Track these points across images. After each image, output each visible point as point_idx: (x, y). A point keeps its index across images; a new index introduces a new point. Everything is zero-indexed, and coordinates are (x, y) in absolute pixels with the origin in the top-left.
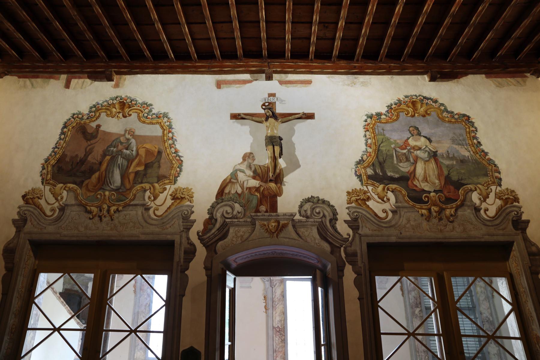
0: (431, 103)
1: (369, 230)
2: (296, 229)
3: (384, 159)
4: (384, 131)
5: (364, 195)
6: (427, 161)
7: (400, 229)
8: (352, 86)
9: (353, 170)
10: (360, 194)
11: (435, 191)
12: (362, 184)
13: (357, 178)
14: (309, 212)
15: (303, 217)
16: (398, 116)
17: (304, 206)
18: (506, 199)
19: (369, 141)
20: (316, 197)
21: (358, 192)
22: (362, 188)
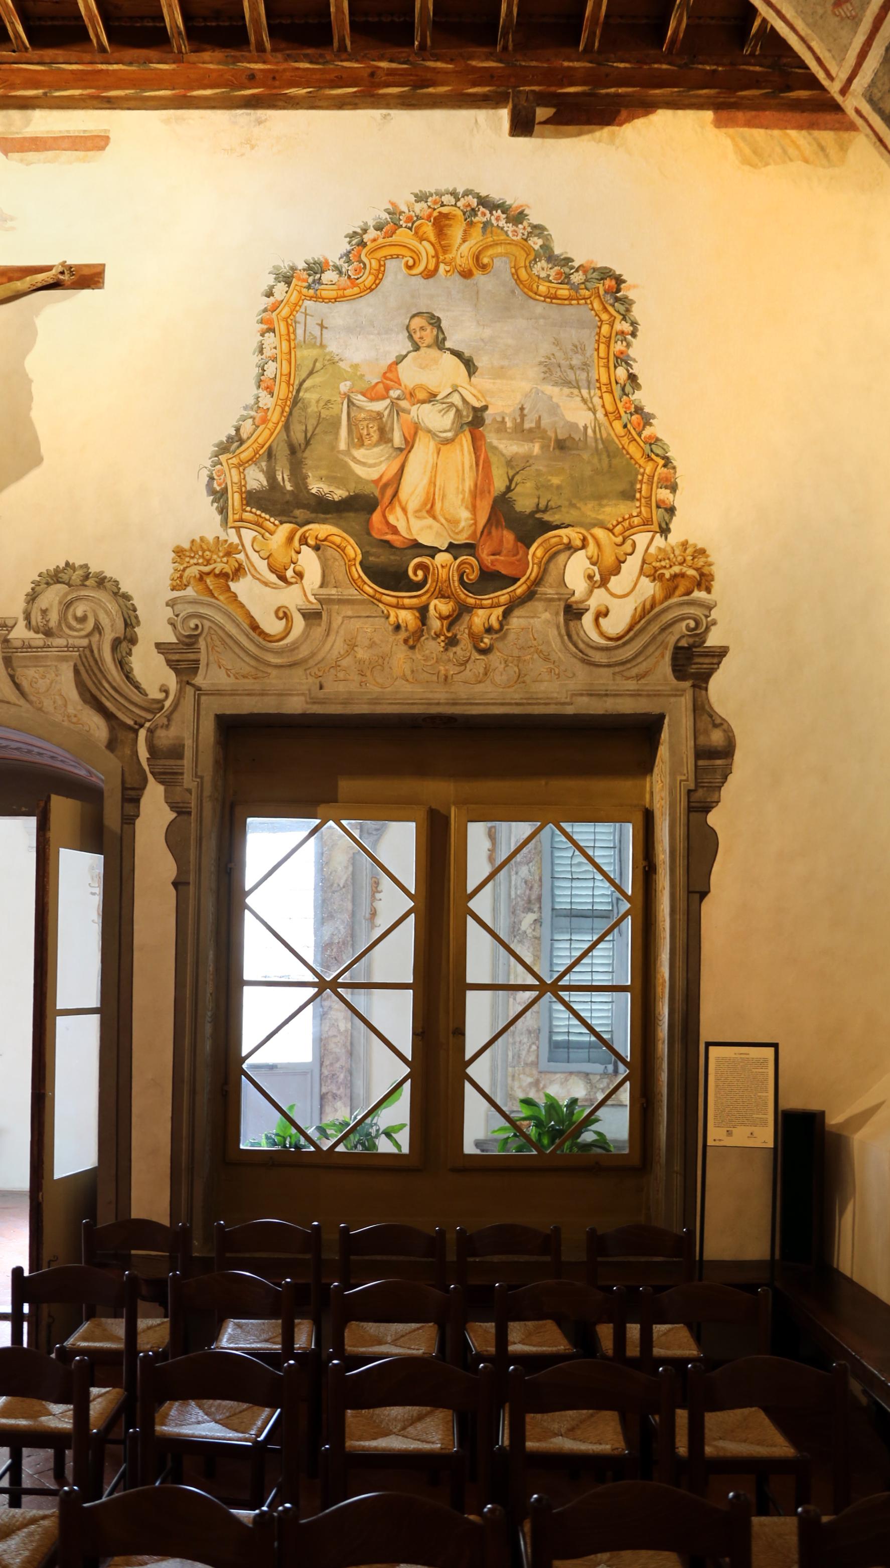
0: (502, 223)
1: (229, 676)
2: (13, 669)
3: (309, 435)
4: (324, 331)
5: (225, 559)
6: (447, 442)
7: (320, 674)
8: (243, 155)
9: (205, 473)
10: (215, 557)
11: (452, 548)
12: (225, 522)
13: (213, 502)
14: (54, 618)
15: (37, 632)
16: (379, 275)
17: (41, 597)
18: (675, 576)
19: (271, 369)
20: (81, 567)
21: (209, 551)
22: (223, 537)
